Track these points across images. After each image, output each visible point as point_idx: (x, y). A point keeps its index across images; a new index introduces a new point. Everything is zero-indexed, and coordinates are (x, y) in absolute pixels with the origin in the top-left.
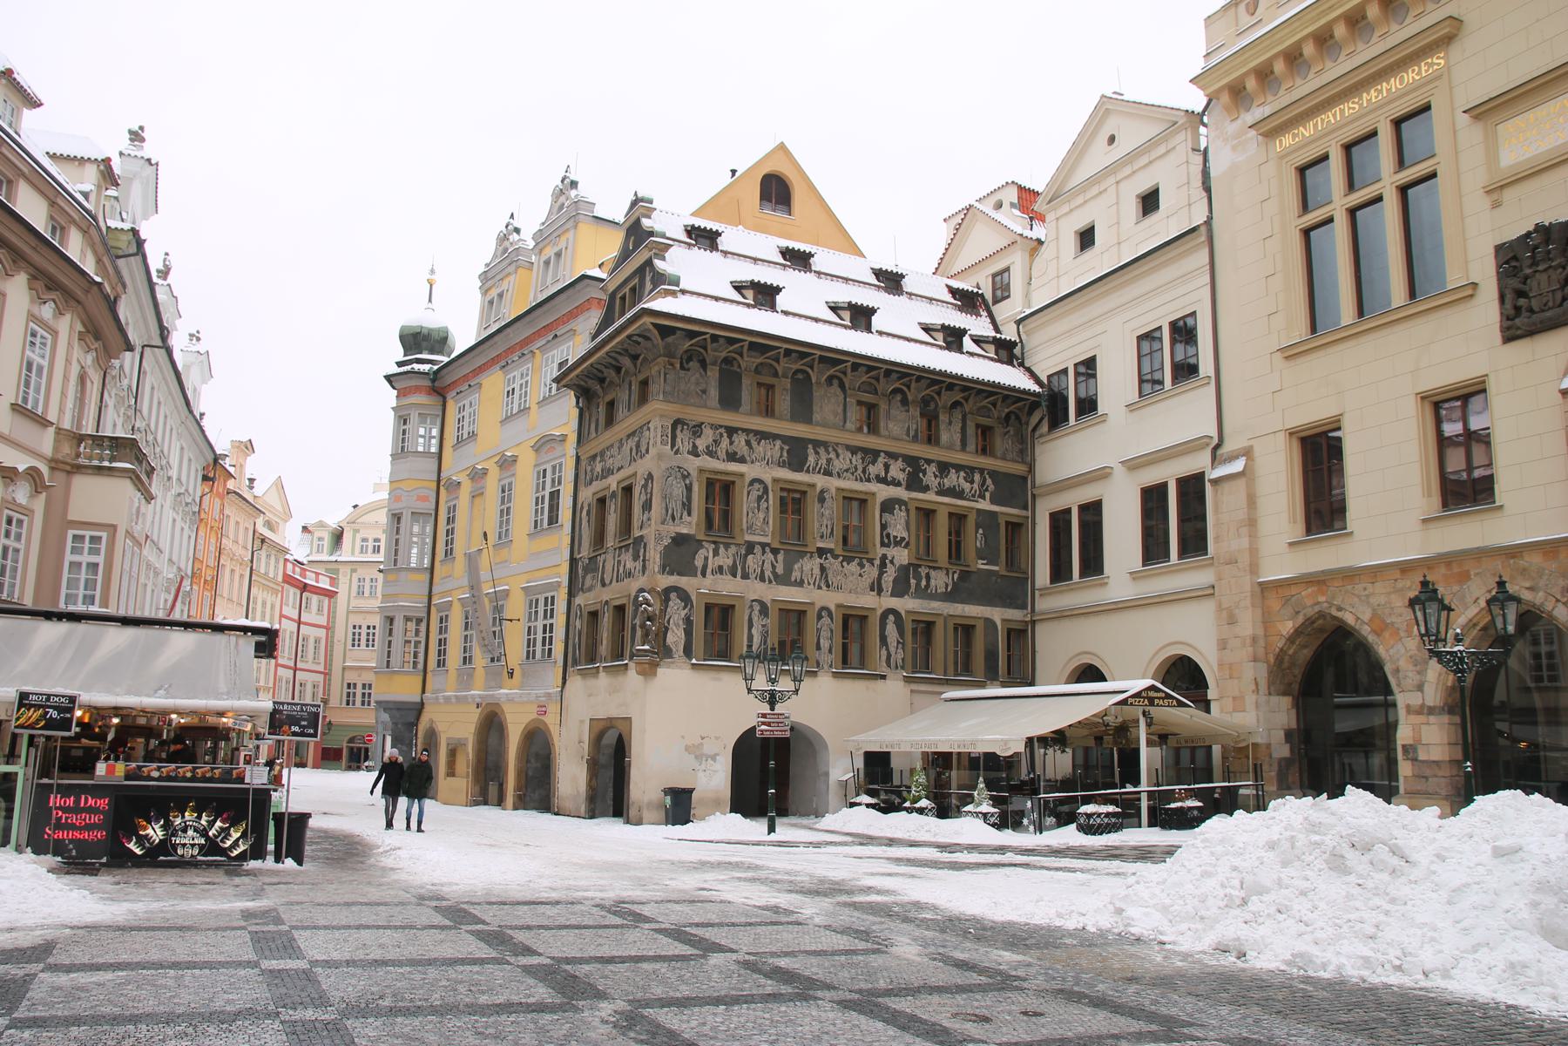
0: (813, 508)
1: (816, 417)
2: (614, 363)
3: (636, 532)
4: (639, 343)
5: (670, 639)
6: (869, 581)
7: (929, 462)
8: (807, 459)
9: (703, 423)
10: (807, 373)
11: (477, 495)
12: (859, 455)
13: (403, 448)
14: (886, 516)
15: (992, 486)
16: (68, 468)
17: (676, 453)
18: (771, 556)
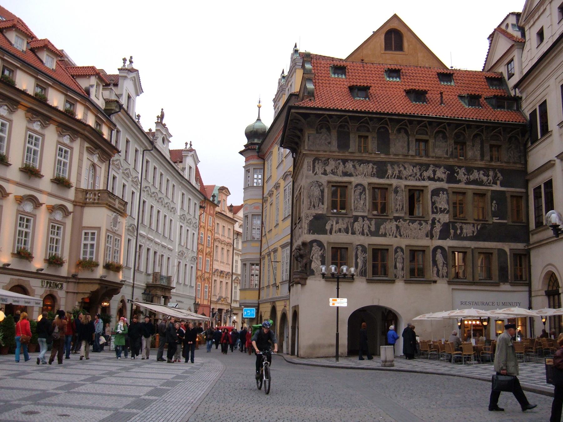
0: (392, 196)
1: (392, 150)
6: (426, 232)
9: (329, 159)
10: (386, 128)
12: (418, 167)
14: (435, 198)
16: (81, 204)
17: (315, 174)
18: (367, 222)
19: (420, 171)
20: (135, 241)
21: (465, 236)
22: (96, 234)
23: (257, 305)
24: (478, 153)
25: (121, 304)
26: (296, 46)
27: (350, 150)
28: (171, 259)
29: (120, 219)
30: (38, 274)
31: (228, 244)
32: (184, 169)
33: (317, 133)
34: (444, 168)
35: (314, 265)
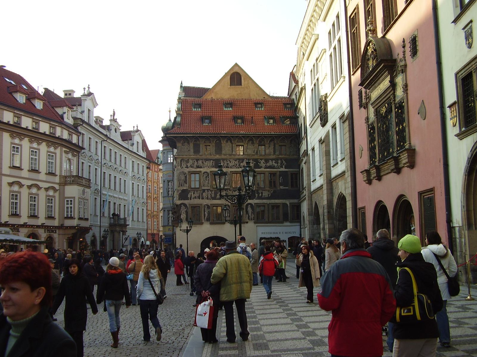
1: (223, 152)
5: (182, 217)
12: (237, 161)
15: (286, 163)
16: (63, 185)
17: (182, 168)
18: (210, 192)
20: (99, 198)
22: (73, 201)
24: (272, 151)
25: (93, 238)
26: (182, 83)
27: (200, 154)
29: (87, 190)
30: (42, 226)
32: (133, 145)
33: (182, 145)
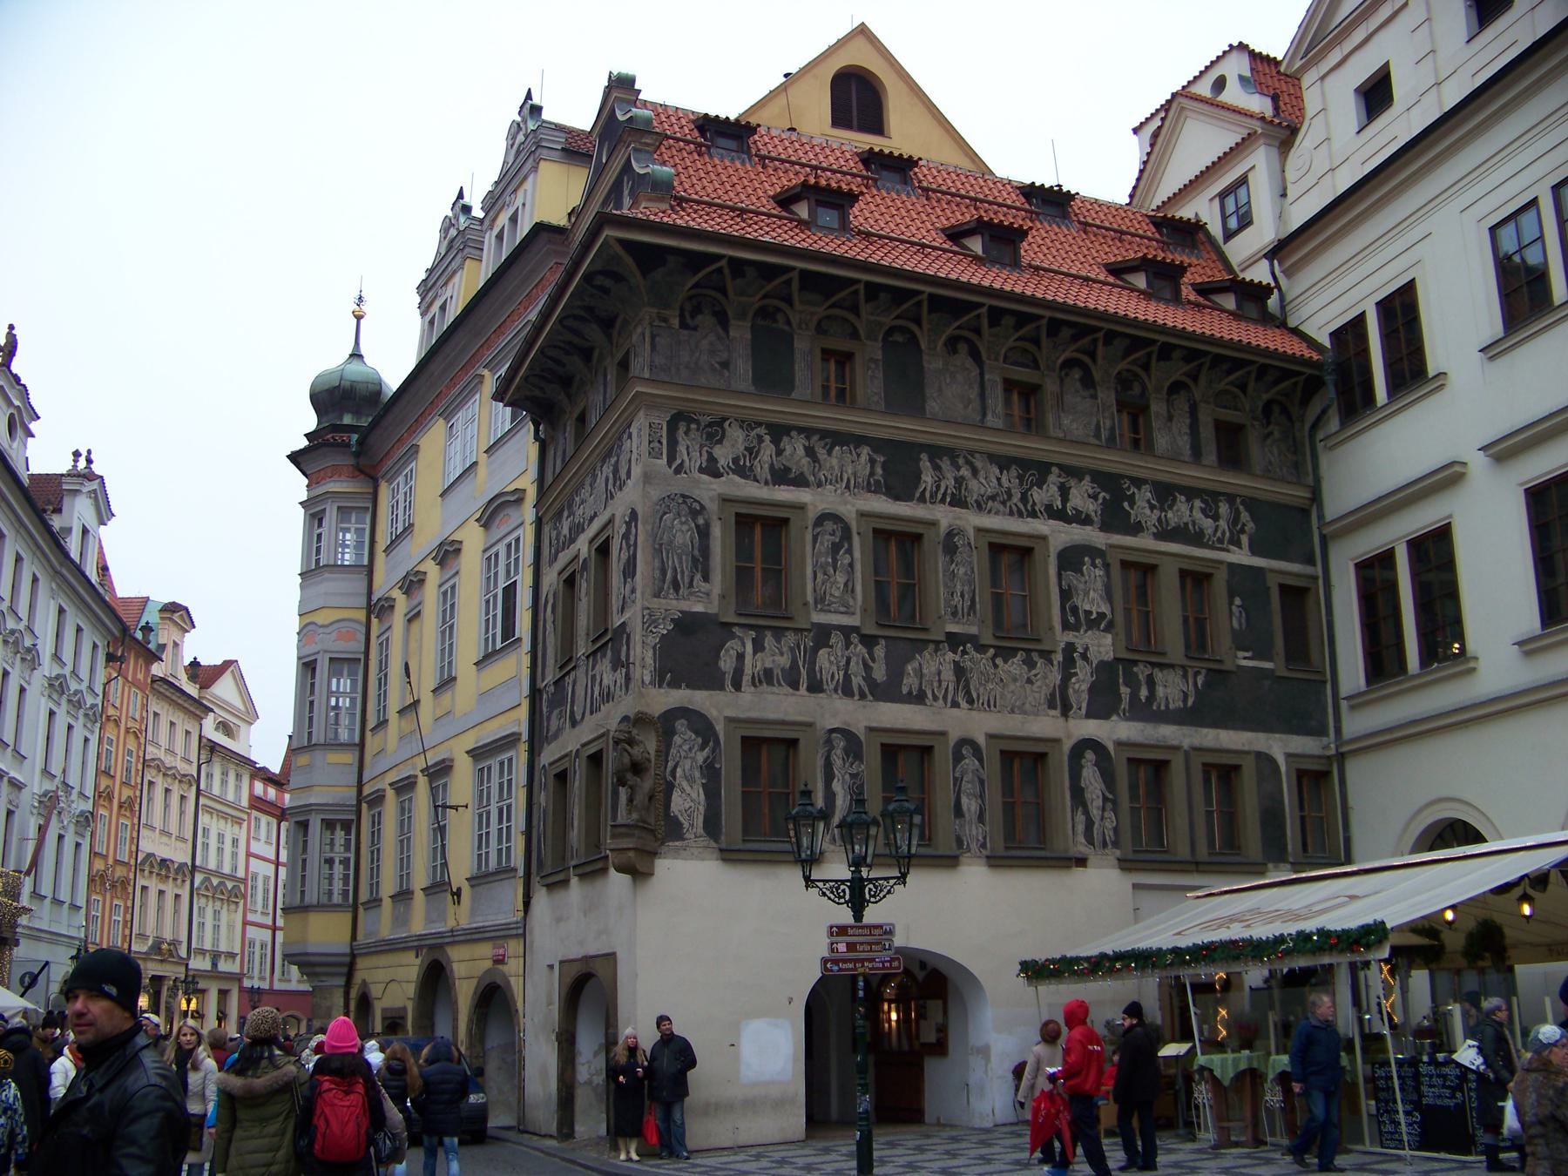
1: (933, 406)
2: (576, 340)
3: (615, 619)
4: (605, 291)
5: (678, 803)
6: (1046, 691)
7: (1138, 482)
8: (919, 478)
9: (724, 419)
10: (911, 332)
11: (414, 617)
12: (1014, 473)
13: (318, 561)
14: (1069, 575)
17: (678, 471)
19: (1021, 484)
21: (1163, 708)
23: (347, 959)
24: (1184, 443)
28: (17, 818)
31: (183, 779)
34: (1093, 481)
35: (680, 801)
